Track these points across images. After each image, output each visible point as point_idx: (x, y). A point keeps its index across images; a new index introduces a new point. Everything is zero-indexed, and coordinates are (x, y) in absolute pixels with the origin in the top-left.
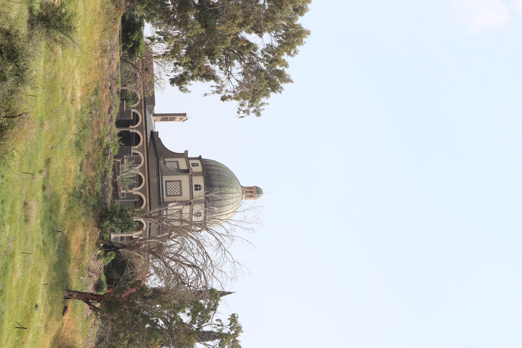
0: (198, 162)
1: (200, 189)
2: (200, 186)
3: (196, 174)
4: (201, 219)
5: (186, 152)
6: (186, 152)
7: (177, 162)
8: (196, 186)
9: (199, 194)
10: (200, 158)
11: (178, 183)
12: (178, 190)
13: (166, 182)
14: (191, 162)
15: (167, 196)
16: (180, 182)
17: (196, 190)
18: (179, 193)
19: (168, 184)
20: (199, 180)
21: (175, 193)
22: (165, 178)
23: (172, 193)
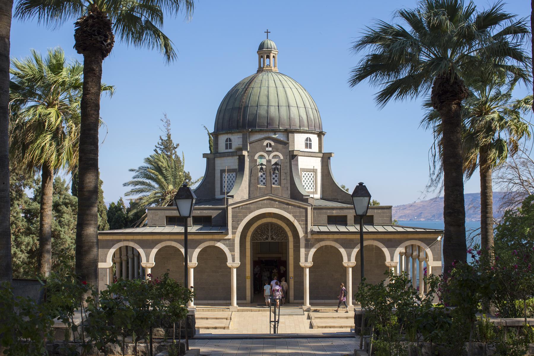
0: (222, 139)
4: (314, 138)
5: (205, 155)
6: (205, 155)
7: (222, 171)
10: (215, 136)
14: (222, 148)
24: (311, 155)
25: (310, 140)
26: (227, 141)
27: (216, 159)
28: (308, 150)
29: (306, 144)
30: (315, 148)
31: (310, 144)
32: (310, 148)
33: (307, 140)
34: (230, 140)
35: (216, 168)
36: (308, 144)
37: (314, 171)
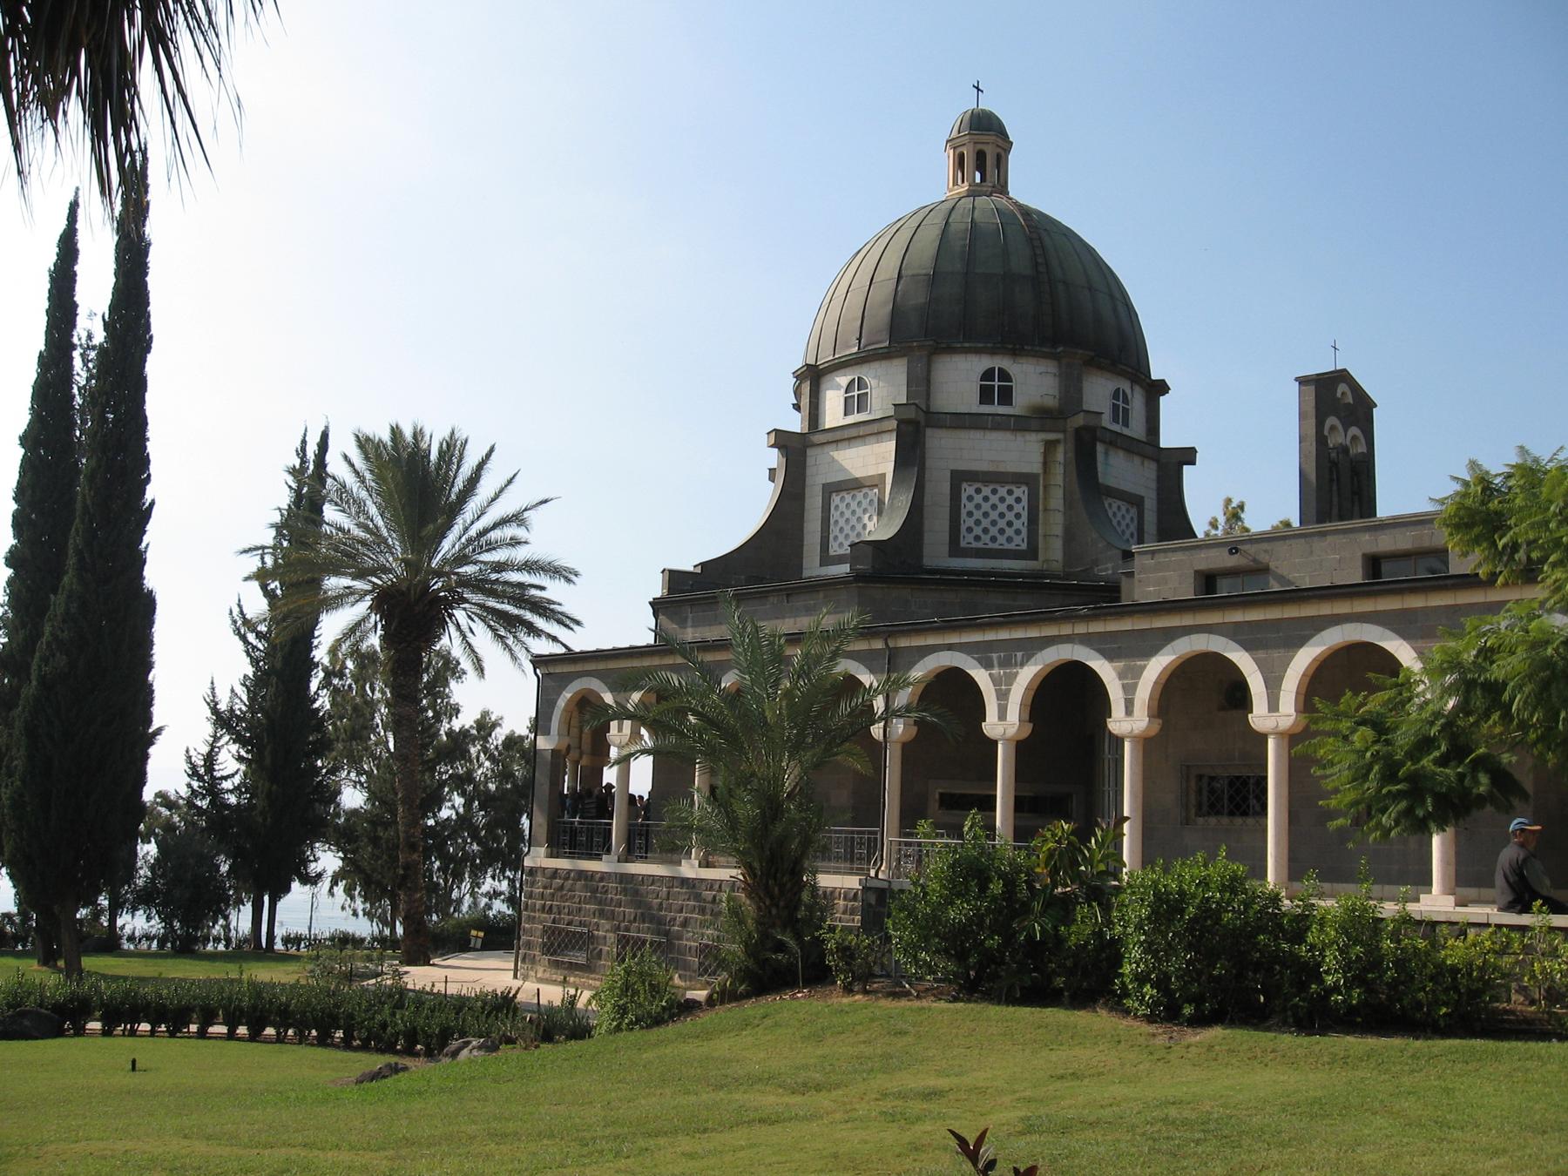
1: (1005, 376)
2: (988, 375)
3: (921, 384)
7: (830, 490)
8: (986, 395)
9: (1034, 381)
10: (812, 377)
11: (968, 489)
12: (1002, 491)
13: (955, 549)
14: (833, 412)
15: (1032, 553)
16: (959, 478)
17: (1006, 396)
18: (1021, 492)
19: (966, 540)
20: (958, 382)
21: (1022, 508)
22: (936, 553)
23: (1021, 524)
24: (1130, 446)
25: (1126, 401)
26: (848, 389)
27: (810, 452)
28: (1117, 428)
29: (1115, 408)
30: (1137, 429)
31: (1126, 411)
32: (1126, 424)
33: (1116, 395)
34: (861, 383)
35: (809, 481)
36: (1120, 414)
37: (1136, 501)
